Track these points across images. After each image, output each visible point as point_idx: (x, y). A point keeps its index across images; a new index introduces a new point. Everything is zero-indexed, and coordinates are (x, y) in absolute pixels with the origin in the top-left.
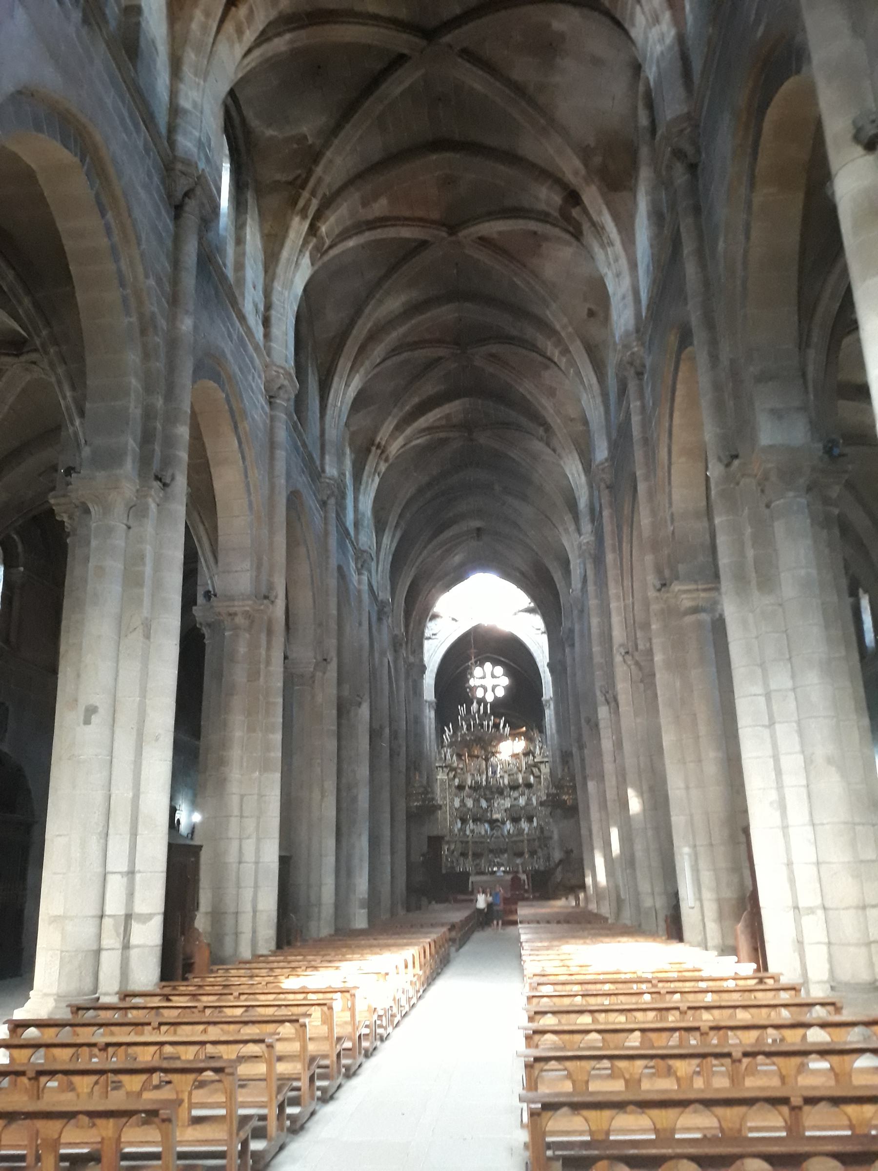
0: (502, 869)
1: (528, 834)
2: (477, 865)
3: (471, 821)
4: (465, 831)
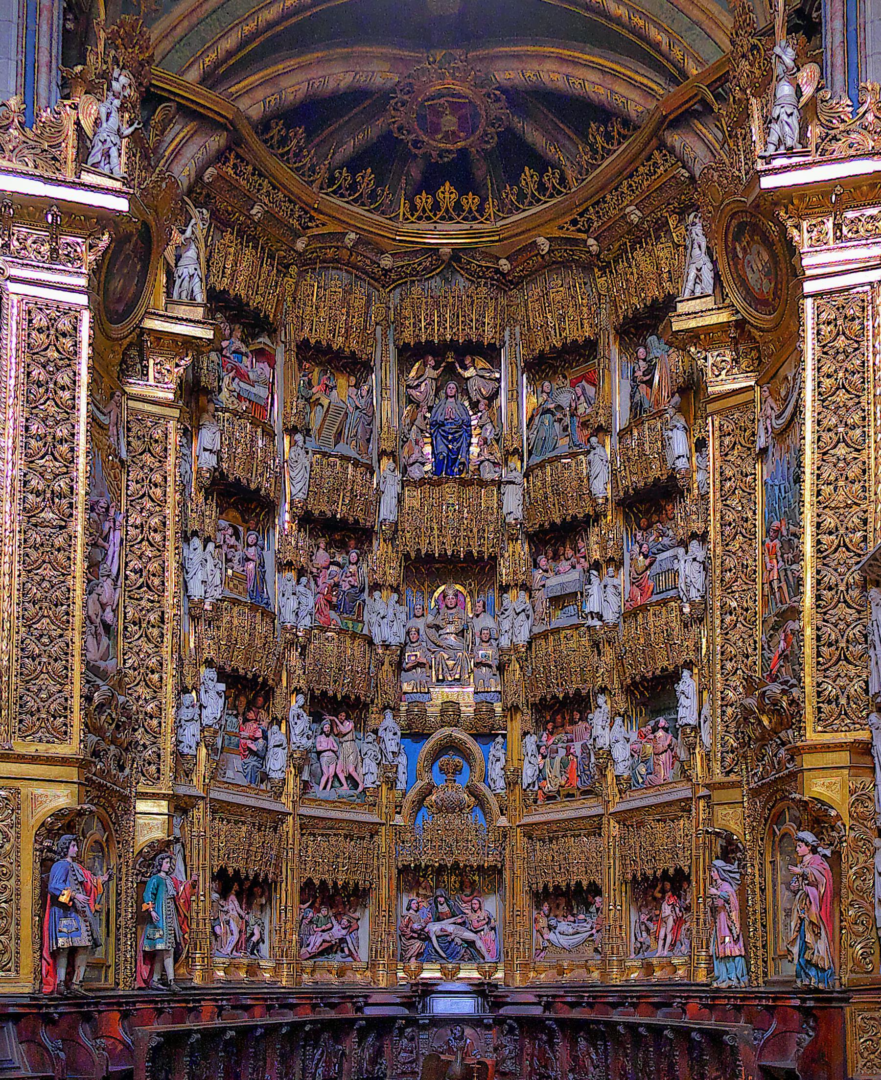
0: (470, 973)
1: (626, 785)
2: (328, 950)
3: (297, 702)
4: (261, 756)
